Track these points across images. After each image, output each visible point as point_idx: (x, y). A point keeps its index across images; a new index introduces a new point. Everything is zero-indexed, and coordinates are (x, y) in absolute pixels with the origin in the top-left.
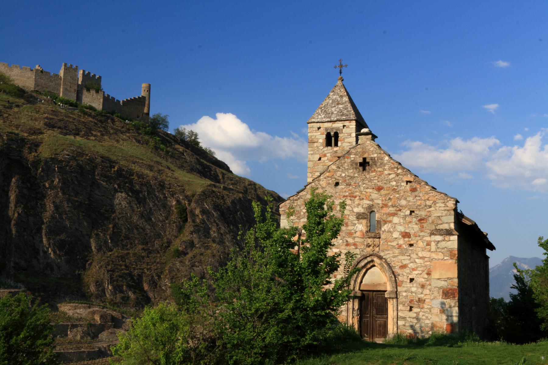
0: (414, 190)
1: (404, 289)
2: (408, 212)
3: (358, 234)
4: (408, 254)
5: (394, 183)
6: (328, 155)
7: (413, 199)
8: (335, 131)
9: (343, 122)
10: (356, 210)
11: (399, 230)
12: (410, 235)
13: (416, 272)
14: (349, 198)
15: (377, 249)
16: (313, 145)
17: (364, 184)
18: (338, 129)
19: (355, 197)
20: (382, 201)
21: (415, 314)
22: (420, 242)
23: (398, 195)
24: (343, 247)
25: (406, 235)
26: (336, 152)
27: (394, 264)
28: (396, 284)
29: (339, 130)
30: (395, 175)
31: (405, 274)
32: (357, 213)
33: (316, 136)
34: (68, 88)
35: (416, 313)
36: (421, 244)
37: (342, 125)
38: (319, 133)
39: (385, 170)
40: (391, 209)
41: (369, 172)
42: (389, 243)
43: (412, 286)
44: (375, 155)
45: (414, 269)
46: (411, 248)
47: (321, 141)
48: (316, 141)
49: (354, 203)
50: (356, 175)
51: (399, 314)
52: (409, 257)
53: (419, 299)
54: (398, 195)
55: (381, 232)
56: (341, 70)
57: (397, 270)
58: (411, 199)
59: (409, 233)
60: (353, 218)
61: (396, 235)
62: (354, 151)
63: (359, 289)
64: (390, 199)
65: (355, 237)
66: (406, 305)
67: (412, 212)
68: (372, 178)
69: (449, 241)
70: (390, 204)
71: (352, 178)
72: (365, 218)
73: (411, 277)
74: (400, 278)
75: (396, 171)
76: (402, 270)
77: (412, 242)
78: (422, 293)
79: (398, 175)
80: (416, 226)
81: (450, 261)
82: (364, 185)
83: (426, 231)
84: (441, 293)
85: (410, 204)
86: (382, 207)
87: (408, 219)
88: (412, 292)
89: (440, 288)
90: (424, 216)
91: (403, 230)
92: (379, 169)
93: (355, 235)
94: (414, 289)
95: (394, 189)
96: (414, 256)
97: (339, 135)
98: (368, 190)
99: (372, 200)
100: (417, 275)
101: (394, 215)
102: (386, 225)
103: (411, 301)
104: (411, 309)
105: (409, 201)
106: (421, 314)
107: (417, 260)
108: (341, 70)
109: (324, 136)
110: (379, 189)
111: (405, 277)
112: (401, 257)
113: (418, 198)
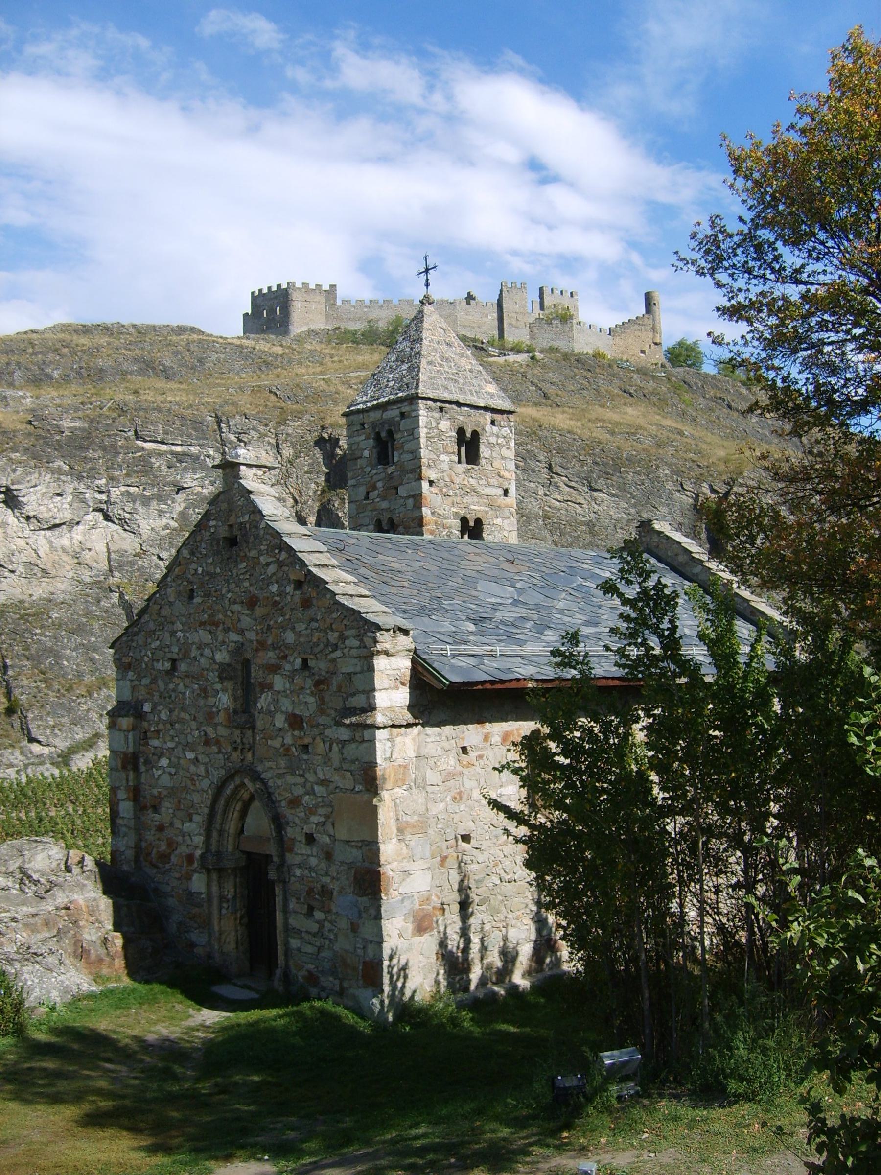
0: (306, 603)
1: (297, 860)
2: (299, 661)
3: (221, 718)
4: (301, 772)
5: (274, 588)
6: (379, 484)
7: (306, 629)
8: (386, 427)
9: (399, 405)
10: (219, 657)
11: (284, 709)
12: (302, 720)
13: (315, 819)
14: (208, 628)
15: (249, 756)
16: (356, 465)
17: (229, 592)
18: (391, 422)
19: (217, 626)
20: (257, 634)
21: (317, 925)
22: (318, 740)
23: (280, 620)
24: (200, 748)
25: (295, 721)
26: (390, 477)
27: (279, 794)
28: (284, 845)
29: (394, 425)
30: (276, 565)
31: (297, 820)
32: (221, 664)
33: (358, 443)
34: (514, 322)
35: (318, 922)
36: (320, 747)
37: (397, 412)
38: (363, 437)
39: (261, 553)
40: (271, 654)
41: (236, 561)
42: (270, 742)
43: (309, 853)
44: (247, 517)
45: (312, 811)
46: (305, 757)
47: (366, 453)
48: (360, 455)
49: (216, 640)
50: (218, 570)
51: (291, 921)
52: (303, 780)
53: (323, 886)
54: (280, 620)
55: (256, 713)
56: (427, 280)
57: (284, 808)
58: (301, 627)
59: (300, 716)
60: (213, 676)
61: (280, 721)
62: (214, 511)
63: (237, 847)
64: (269, 628)
65: (216, 725)
66: (302, 900)
67: (305, 661)
68: (241, 577)
69: (363, 741)
70: (269, 642)
71: (212, 576)
72: (230, 678)
73: (307, 829)
74: (290, 832)
75: (277, 556)
76: (293, 811)
77: (306, 741)
78: (327, 874)
79: (280, 564)
80: (311, 700)
81: (366, 797)
82: (229, 595)
83: (328, 711)
84: (352, 879)
85: (302, 640)
86: (257, 650)
87: (298, 680)
88: (311, 869)
89: (350, 866)
90: (323, 673)
91: (290, 710)
92: (253, 553)
93: (216, 720)
94: (313, 861)
95: (276, 603)
96: (311, 777)
97: (397, 436)
98: (236, 607)
99: (241, 632)
100: (317, 824)
101: (274, 669)
102: (263, 697)
103: (310, 891)
104: (311, 909)
105: (299, 634)
106: (326, 924)
107: (316, 787)
108: (427, 280)
109: (371, 442)
110: (252, 603)
111: (298, 829)
112: (290, 779)
113: (314, 625)
